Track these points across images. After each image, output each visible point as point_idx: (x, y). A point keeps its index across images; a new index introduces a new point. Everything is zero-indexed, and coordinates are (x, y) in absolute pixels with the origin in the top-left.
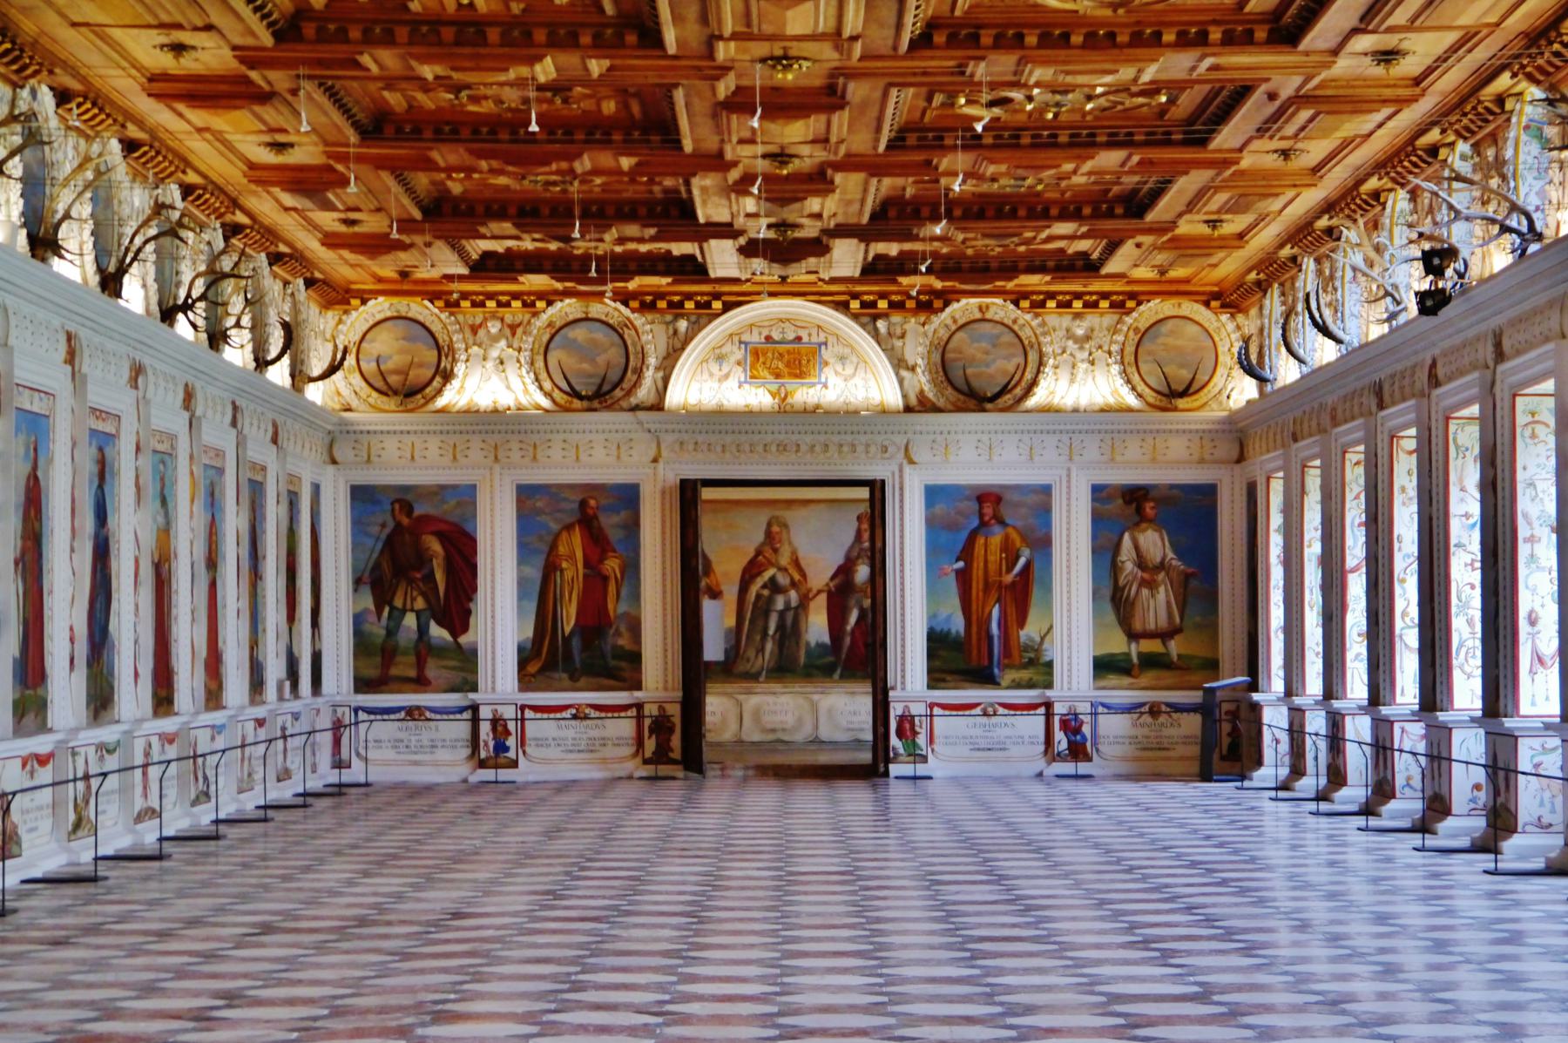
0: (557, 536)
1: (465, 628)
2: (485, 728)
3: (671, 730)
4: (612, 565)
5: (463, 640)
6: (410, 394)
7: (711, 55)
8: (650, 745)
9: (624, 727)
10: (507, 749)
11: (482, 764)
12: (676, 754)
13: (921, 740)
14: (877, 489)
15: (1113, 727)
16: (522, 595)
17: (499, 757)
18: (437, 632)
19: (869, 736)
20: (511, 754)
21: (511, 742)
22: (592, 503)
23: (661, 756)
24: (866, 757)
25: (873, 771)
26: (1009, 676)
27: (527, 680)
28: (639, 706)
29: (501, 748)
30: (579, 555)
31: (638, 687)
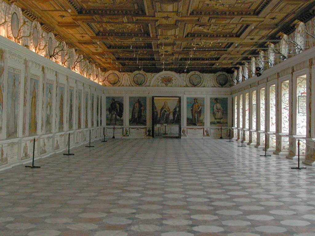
0: (135, 104)
1: (122, 117)
2: (124, 131)
3: (151, 131)
4: (142, 108)
5: (122, 118)
6: (114, 84)
7: (157, 37)
8: (148, 133)
9: (143, 130)
10: (127, 134)
11: (124, 136)
12: (151, 135)
13: (186, 133)
14: (180, 98)
15: (212, 131)
16: (130, 112)
17: (126, 135)
18: (118, 117)
19: (178, 132)
20: (128, 134)
21: (128, 133)
22: (140, 99)
23: (149, 135)
24: (177, 135)
25: (179, 137)
26: (198, 124)
27: (130, 124)
28: (146, 128)
29: (126, 133)
30: (138, 107)
31: (146, 125)
